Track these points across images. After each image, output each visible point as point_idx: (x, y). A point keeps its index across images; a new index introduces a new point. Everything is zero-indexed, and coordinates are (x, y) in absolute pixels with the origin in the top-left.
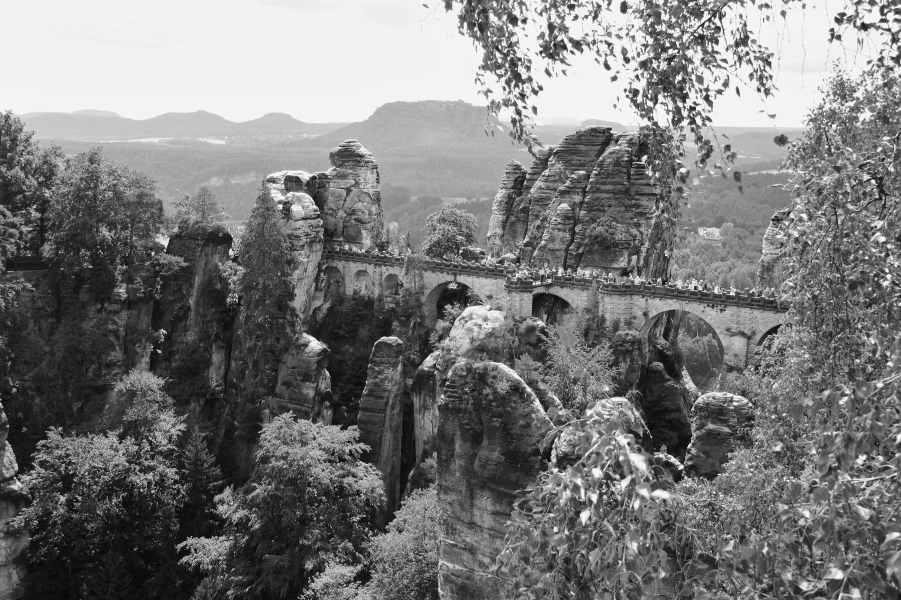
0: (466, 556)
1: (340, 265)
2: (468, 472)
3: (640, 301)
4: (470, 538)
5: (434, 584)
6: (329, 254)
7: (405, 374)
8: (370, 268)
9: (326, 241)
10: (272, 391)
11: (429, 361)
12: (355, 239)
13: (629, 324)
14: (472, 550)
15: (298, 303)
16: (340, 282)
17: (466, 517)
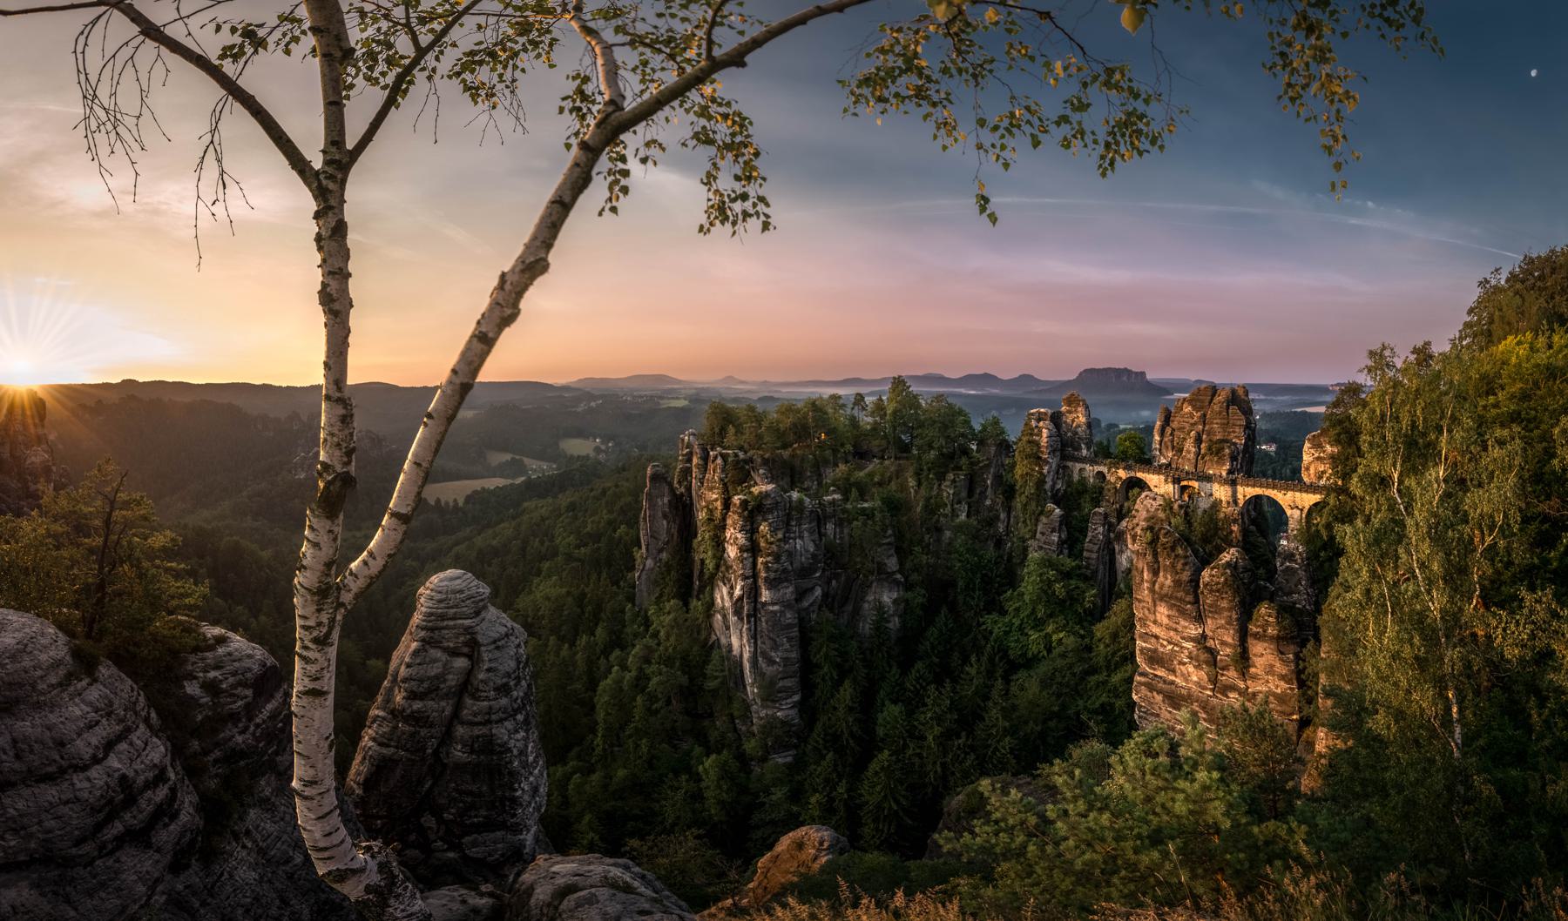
0: (1153, 640)
1: (1070, 464)
2: (1152, 590)
3: (1240, 489)
4: (1155, 630)
5: (1133, 655)
6: (1064, 457)
7: (1109, 531)
8: (1088, 467)
9: (1062, 451)
10: (1034, 537)
11: (1124, 523)
12: (1079, 449)
13: (1235, 502)
14: (1157, 637)
15: (1047, 487)
16: (1070, 476)
17: (1152, 617)
